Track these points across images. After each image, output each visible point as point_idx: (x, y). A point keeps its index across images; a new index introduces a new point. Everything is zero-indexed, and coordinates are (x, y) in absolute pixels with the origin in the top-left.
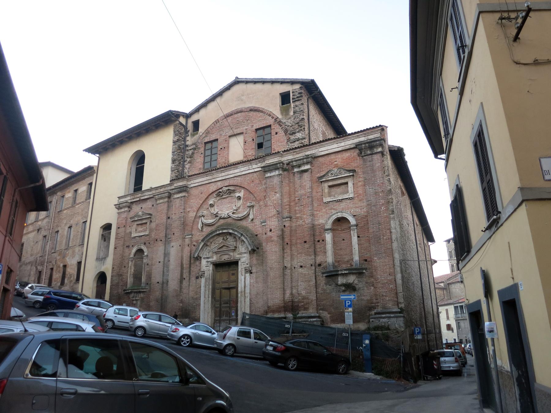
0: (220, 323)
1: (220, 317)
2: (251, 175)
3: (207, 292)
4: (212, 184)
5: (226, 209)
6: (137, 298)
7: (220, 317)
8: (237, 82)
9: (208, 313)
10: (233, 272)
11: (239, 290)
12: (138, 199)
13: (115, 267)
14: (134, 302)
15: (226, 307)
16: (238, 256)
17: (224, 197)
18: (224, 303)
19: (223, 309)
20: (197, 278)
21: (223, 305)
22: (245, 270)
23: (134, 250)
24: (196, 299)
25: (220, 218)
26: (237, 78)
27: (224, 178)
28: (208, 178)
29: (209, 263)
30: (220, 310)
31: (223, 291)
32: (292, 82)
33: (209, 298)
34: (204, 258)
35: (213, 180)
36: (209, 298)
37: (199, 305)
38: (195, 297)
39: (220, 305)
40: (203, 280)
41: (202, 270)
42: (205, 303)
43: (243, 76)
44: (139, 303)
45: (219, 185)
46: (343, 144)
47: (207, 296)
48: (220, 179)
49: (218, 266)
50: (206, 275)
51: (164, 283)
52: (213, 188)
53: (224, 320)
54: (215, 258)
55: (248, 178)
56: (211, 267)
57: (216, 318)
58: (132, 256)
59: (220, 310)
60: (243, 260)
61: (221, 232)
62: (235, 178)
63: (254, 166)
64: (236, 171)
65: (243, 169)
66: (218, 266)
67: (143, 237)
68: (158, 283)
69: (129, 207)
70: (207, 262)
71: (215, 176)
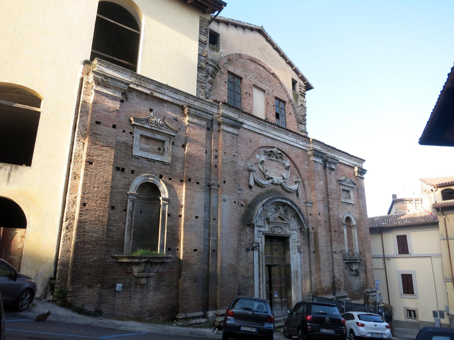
2: (297, 149)
4: (261, 136)
5: (277, 173)
6: (151, 274)
8: (261, 31)
12: (149, 92)
13: (91, 204)
14: (144, 281)
16: (289, 232)
17: (272, 158)
20: (248, 250)
23: (138, 181)
24: (248, 278)
25: (272, 183)
26: (262, 27)
27: (275, 138)
28: (259, 127)
32: (303, 78)
35: (264, 133)
37: (253, 286)
38: (246, 275)
40: (256, 253)
43: (268, 31)
44: (152, 282)
45: (276, 144)
46: (349, 161)
48: (272, 136)
51: (210, 252)
52: (263, 142)
55: (295, 150)
58: (133, 190)
60: (293, 237)
61: (280, 200)
62: (283, 144)
63: (301, 143)
64: (287, 137)
65: (292, 139)
67: (157, 164)
68: (195, 250)
69: (124, 94)
71: (267, 130)
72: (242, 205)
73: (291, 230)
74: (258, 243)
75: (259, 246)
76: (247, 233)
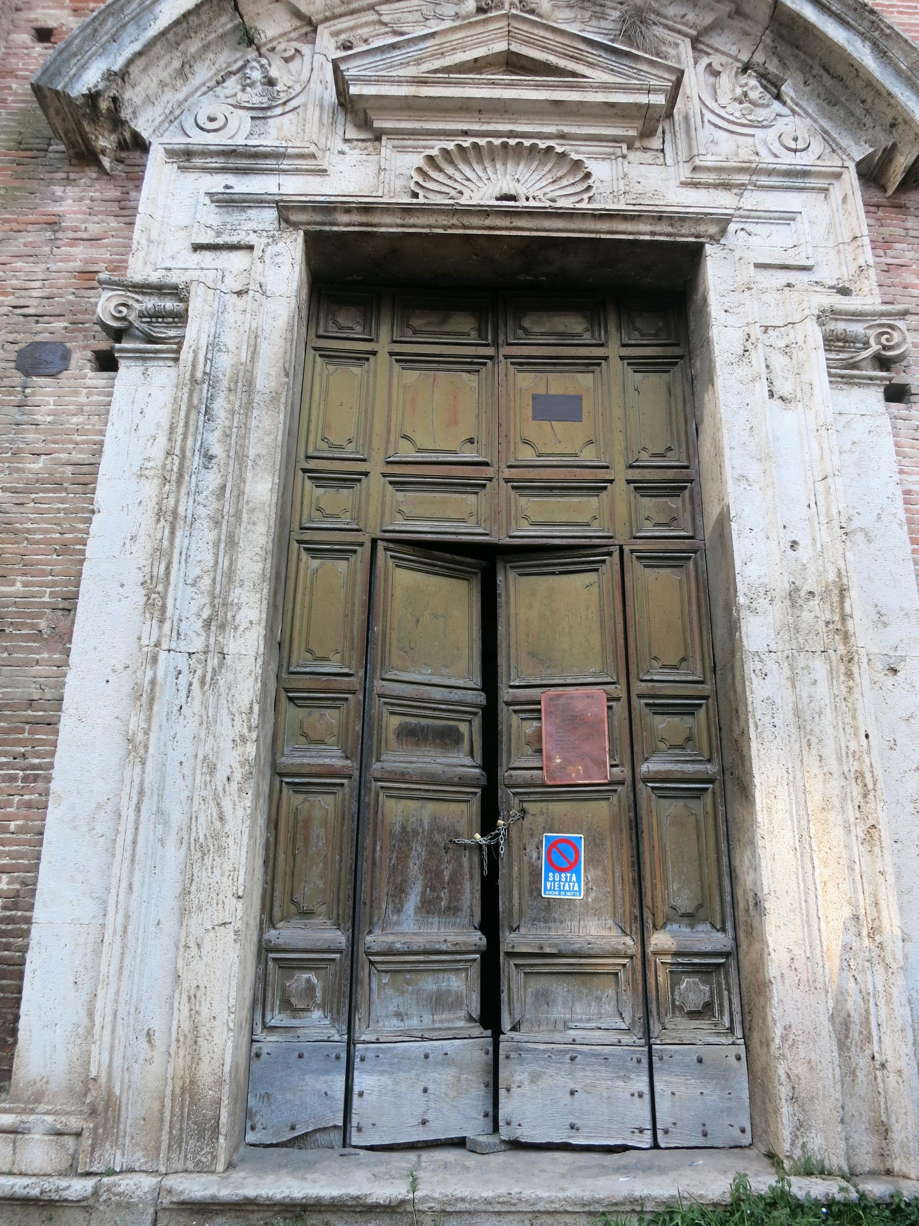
0: (348, 1004)
1: (355, 915)
3: (199, 547)
7: (355, 915)
9: (202, 848)
10: (558, 384)
11: (757, 562)
15: (433, 787)
18: (412, 735)
19: (396, 811)
21: (397, 758)
22: (832, 342)
29: (271, 215)
30: (360, 823)
31: (405, 582)
33: (218, 620)
34: (185, 157)
36: (218, 620)
39: (364, 747)
40: (143, 395)
41: (139, 270)
42: (146, 697)
47: (188, 604)
49: (365, 278)
50: (196, 332)
53: (411, 963)
54: (357, 175)
56: (284, 269)
57: (288, 934)
59: (360, 823)
66: (365, 278)
70: (228, 202)
72: (44, 35)
73: (725, 179)
74: (177, 292)
75: (181, 318)
76: (53, 224)
